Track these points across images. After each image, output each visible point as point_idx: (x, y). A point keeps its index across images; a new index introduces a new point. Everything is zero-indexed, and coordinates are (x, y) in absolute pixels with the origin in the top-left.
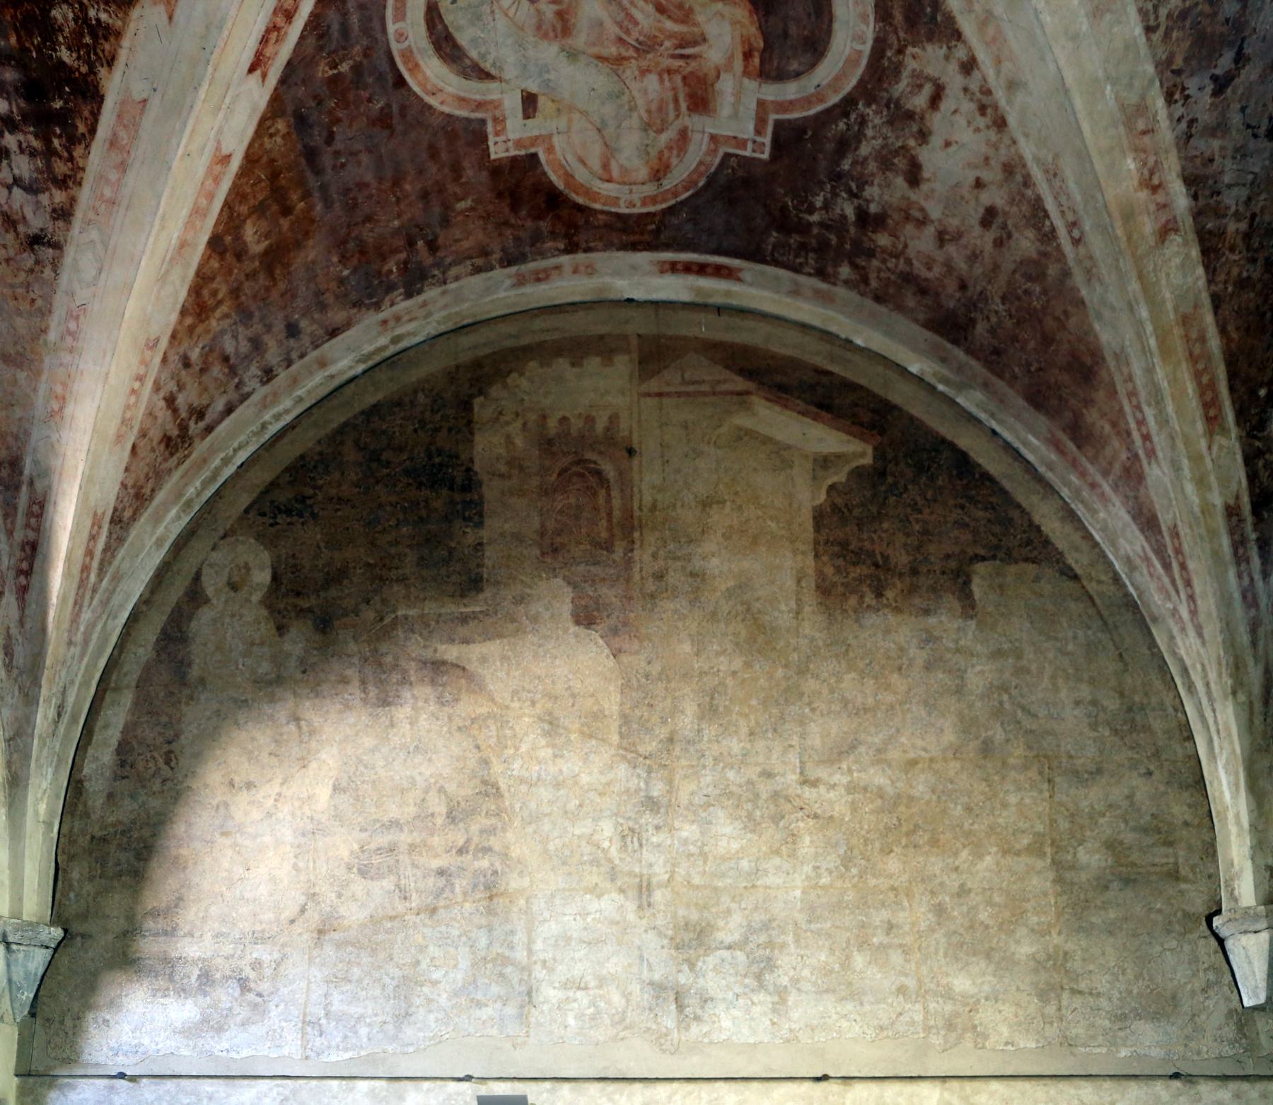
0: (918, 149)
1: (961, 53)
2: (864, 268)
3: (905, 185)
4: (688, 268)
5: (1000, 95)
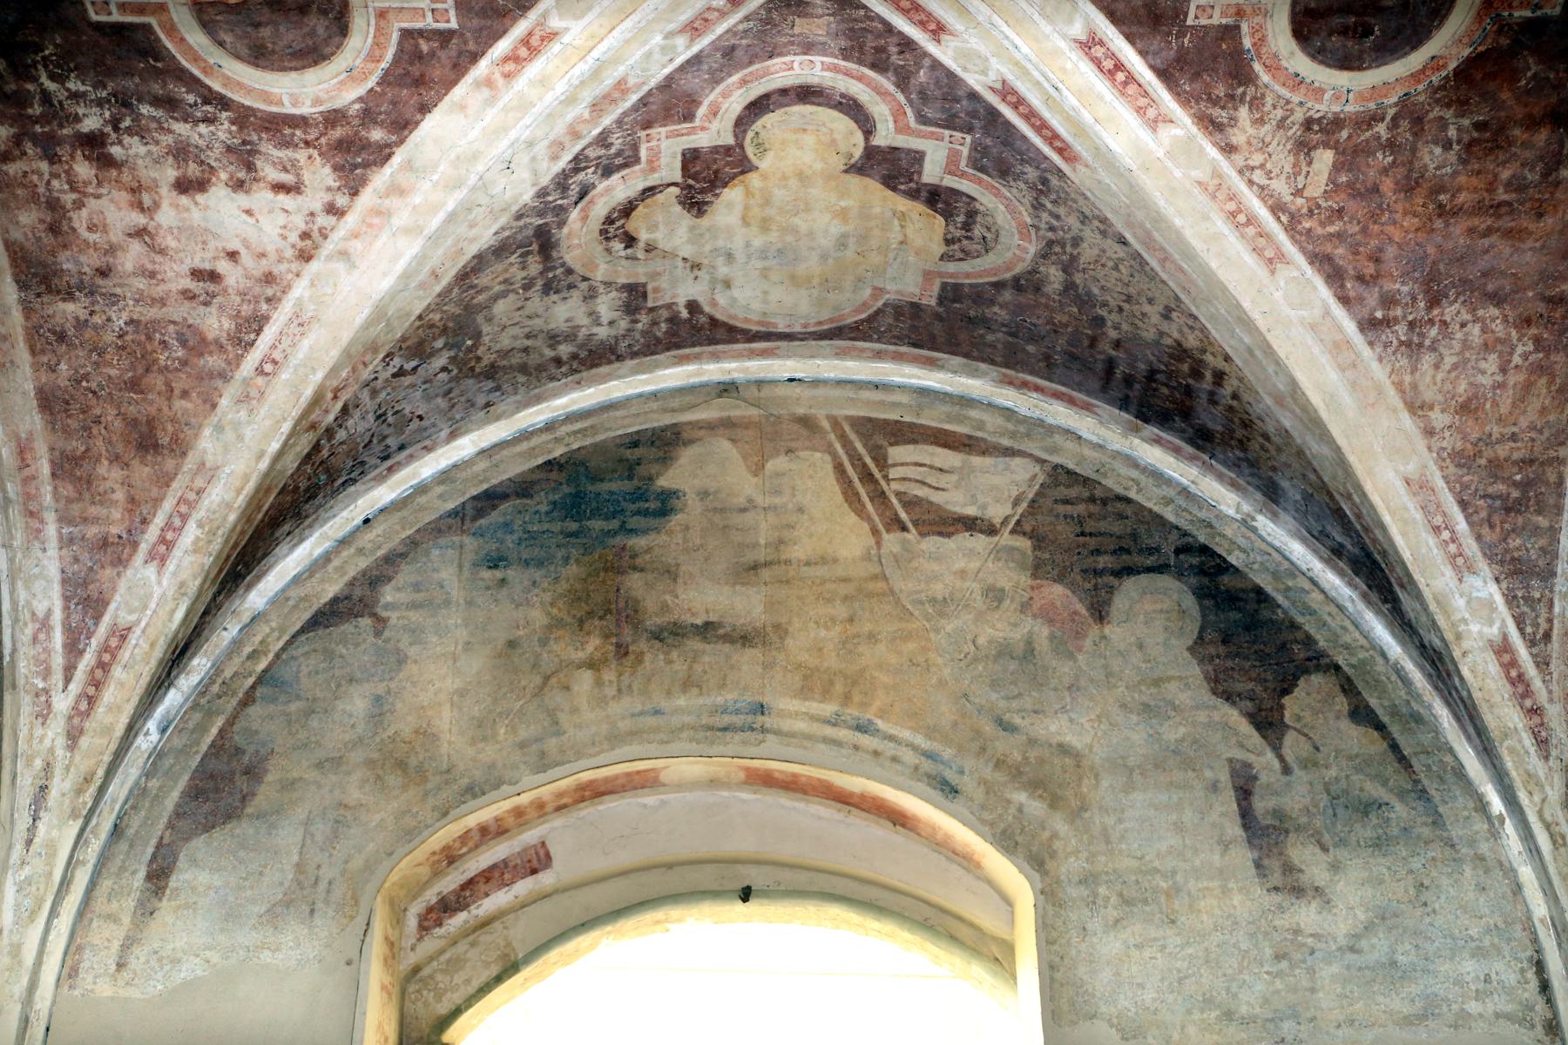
0: (222, 185)
1: (341, 200)
3: (172, 180)
5: (328, 247)
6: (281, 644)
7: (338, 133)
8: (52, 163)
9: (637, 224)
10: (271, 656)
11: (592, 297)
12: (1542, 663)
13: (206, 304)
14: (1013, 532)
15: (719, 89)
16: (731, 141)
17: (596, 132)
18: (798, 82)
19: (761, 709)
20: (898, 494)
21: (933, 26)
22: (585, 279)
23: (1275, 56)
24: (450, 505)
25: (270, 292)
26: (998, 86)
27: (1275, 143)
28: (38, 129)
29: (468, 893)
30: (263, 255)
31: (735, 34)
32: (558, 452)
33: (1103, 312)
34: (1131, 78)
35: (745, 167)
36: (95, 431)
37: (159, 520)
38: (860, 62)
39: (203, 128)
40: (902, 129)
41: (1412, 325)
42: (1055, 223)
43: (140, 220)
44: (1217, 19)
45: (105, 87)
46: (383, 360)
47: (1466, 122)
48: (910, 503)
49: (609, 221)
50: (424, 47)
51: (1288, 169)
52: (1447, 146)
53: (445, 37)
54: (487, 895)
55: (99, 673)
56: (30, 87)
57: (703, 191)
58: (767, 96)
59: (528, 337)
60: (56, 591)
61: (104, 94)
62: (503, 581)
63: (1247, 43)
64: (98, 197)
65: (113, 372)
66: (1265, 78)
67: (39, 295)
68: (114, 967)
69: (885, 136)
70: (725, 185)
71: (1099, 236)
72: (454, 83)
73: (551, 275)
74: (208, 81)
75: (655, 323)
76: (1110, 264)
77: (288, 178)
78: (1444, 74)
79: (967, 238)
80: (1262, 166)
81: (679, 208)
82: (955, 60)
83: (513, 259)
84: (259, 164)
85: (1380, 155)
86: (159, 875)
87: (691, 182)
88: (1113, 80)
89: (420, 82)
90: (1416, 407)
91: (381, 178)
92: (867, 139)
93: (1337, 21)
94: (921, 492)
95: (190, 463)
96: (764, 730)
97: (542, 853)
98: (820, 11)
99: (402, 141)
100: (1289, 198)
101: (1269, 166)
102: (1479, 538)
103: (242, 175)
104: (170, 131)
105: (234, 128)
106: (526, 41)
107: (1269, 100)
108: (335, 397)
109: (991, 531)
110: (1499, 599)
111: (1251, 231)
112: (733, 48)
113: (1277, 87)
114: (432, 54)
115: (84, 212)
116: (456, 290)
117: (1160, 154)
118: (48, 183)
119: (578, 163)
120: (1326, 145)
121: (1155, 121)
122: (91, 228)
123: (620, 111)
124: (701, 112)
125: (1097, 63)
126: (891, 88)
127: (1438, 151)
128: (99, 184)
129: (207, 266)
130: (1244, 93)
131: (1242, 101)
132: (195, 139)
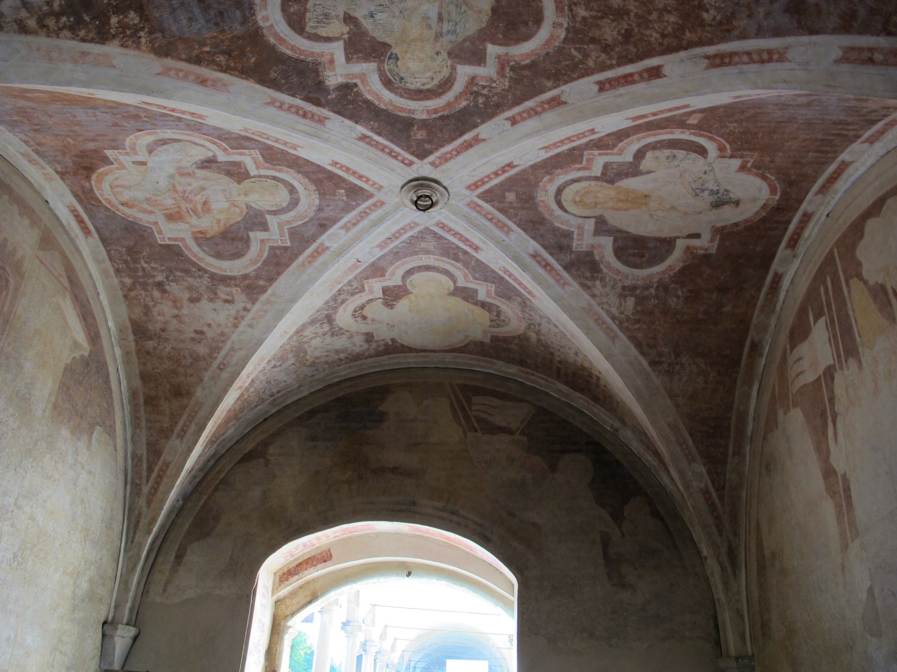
2: (136, 288)
4: (77, 217)
5: (244, 323)
6: (230, 467)
7: (247, 282)
8: (145, 291)
9: (366, 312)
10: (225, 472)
11: (351, 337)
12: (721, 498)
13: (199, 342)
14: (520, 434)
15: (393, 266)
16: (400, 283)
17: (346, 281)
18: (425, 264)
19: (414, 503)
20: (475, 417)
22: (348, 331)
23: (609, 263)
24: (297, 415)
25: (223, 339)
27: (611, 294)
28: (141, 280)
29: (299, 568)
30: (220, 325)
31: (398, 248)
32: (341, 394)
33: (553, 350)
34: (552, 268)
35: (407, 292)
36: (159, 388)
37: (181, 423)
38: (449, 258)
39: (198, 280)
41: (669, 365)
42: (530, 317)
43: (176, 312)
44: (584, 249)
45: (163, 266)
46: (267, 363)
47: (685, 290)
48: (480, 420)
49: (355, 311)
50: (278, 252)
51: (617, 303)
52: (678, 297)
54: (306, 569)
55: (158, 480)
56: (138, 266)
57: (392, 301)
58: (413, 268)
59: (327, 352)
60: (144, 447)
61: (164, 268)
62: (316, 446)
63: (597, 258)
64: (161, 303)
65: (166, 366)
66: (605, 270)
67: (141, 338)
68: (161, 591)
69: (461, 283)
70: (401, 298)
73: (333, 330)
74: (200, 264)
75: (378, 346)
77: (229, 298)
78: (674, 271)
79: (498, 320)
81: (383, 306)
83: (317, 325)
84: (218, 293)
85: (653, 300)
86: (179, 557)
87: (386, 297)
89: (278, 264)
90: (672, 395)
91: (263, 298)
93: (631, 251)
94: (484, 416)
95: (192, 402)
96: (414, 512)
97: (329, 554)
99: (271, 285)
101: (610, 303)
102: (697, 448)
103: (212, 296)
104: (186, 281)
105: (209, 280)
106: (316, 251)
107: (607, 279)
108: (248, 377)
109: (511, 433)
110: (704, 472)
111: (604, 326)
112: (398, 253)
113: (610, 274)
115: (157, 309)
116: (295, 337)
118: (144, 298)
120: (631, 296)
121: (564, 284)
122: (159, 315)
123: (355, 274)
124: (387, 274)
125: (539, 263)
126: (462, 267)
127: (675, 299)
128: (162, 299)
129: (200, 329)
130: (598, 276)
131: (597, 278)
132: (195, 284)
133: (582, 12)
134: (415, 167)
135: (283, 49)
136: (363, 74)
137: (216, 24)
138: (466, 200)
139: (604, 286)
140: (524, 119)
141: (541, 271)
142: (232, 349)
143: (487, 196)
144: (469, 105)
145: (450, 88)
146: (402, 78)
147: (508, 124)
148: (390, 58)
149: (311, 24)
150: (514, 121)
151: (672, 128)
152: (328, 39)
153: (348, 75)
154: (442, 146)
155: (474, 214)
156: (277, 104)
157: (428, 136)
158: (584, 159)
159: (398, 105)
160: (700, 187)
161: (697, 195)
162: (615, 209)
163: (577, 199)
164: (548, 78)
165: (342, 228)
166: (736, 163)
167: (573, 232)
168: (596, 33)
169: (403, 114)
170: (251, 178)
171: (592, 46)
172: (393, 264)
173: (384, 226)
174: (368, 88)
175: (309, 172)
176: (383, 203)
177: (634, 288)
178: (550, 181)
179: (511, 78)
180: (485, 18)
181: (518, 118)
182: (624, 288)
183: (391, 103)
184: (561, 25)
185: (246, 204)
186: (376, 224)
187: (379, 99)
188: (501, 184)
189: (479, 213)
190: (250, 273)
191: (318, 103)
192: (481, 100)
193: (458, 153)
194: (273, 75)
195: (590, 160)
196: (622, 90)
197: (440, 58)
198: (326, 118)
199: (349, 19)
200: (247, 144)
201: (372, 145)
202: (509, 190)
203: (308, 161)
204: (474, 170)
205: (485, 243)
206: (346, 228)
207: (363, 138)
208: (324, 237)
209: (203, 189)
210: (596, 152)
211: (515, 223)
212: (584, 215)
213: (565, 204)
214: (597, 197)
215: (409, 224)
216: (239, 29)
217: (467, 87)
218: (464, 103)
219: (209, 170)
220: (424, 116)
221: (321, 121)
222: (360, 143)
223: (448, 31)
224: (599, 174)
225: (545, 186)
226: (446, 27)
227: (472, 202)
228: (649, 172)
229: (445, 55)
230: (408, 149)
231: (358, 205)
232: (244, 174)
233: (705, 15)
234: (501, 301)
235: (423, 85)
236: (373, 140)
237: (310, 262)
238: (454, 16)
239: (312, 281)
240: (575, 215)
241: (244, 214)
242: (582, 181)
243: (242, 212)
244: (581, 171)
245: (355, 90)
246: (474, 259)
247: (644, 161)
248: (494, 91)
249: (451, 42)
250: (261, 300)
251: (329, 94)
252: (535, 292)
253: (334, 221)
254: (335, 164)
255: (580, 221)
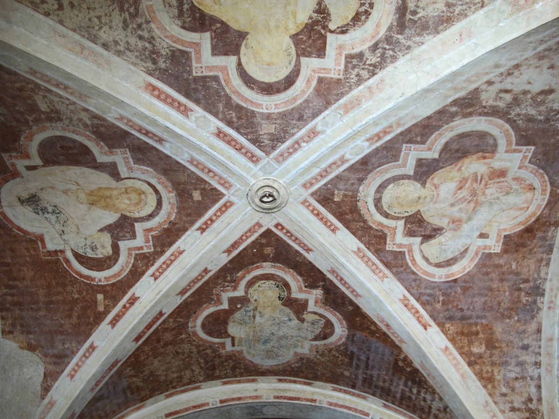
15: (306, 97)
16: (303, 60)
17: (361, 87)
21: (221, 135)
23: (89, 140)
26: (189, 113)
31: (298, 127)
38: (247, 110)
40: (224, 69)
42: (140, 32)
50: (419, 139)
53: (410, 141)
58: (286, 89)
63: (102, 143)
71: (117, 39)
72: (413, 125)
76: (103, 20)
77: (502, 95)
80: (67, 105)
82: (210, 121)
83: (421, 14)
88: (146, 130)
92: (239, 59)
93: (75, 151)
98: (265, 137)
99: (444, 107)
100: (47, 94)
105: (511, 112)
106: (379, 138)
114: (417, 136)
117: (113, 108)
119: (374, 70)
123: (349, 96)
124: (314, 83)
125: (154, 135)
126: (233, 96)
130: (92, 128)
131: (91, 126)
133: (183, 336)
134: (274, 222)
135: (340, 317)
136: (300, 292)
137: (367, 340)
138: (233, 191)
139: (80, 120)
140: (200, 275)
141: (150, 128)
142: (542, 42)
143: (215, 196)
144: (236, 274)
145: (248, 282)
146: (277, 287)
147: (209, 268)
148: (283, 299)
149: (322, 322)
150: (206, 271)
151: (108, 285)
152: (315, 313)
153: (309, 293)
154: (253, 242)
155: (225, 176)
156: (355, 293)
157: (263, 250)
158: (151, 242)
159: (281, 271)
160: (58, 215)
161: (55, 206)
162: (110, 188)
163: (143, 196)
164: (191, 302)
165: (347, 161)
166: (51, 246)
167: (135, 164)
168: (173, 333)
169: (279, 265)
170: (406, 217)
171: (173, 326)
172: (306, 101)
173: (306, 162)
174: (299, 284)
175: (357, 222)
176: (305, 186)
177: (50, 119)
178: (169, 215)
179: (212, 295)
180: (231, 319)
181: (204, 274)
182: (60, 120)
183: (286, 272)
184: (192, 328)
185: (424, 187)
186: (315, 164)
187: (293, 276)
188: (207, 209)
189: (221, 178)
190: (460, 119)
191: (331, 281)
192: (229, 278)
193: (241, 238)
194: (351, 308)
195: (147, 241)
196: (150, 320)
197: (255, 297)
198: (329, 271)
199: (302, 321)
200: (390, 258)
201: (303, 243)
202: (199, 202)
203: (354, 234)
204: (229, 224)
205: (212, 147)
206: (343, 160)
207: (308, 250)
208: (367, 152)
209: (452, 205)
210: (145, 250)
211: (188, 169)
212: (132, 180)
213: (151, 190)
214: (129, 199)
215: (284, 160)
216: (359, 334)
217: (238, 284)
218: (239, 274)
219: (435, 227)
220: (265, 264)
221: (333, 271)
222: (311, 247)
223: (250, 311)
224: (136, 225)
225: (172, 208)
226: (251, 314)
227: (227, 188)
228: (101, 230)
229: (252, 300)
230: (279, 239)
231: (326, 185)
232: (409, 222)
233: (130, 368)
234: (183, 43)
235: (264, 283)
236: (302, 247)
237: (391, 127)
238: (247, 318)
239: (398, 108)
240: (139, 180)
241: (432, 177)
242: (146, 217)
243: (433, 179)
244: (150, 227)
245: (307, 284)
246: (220, 116)
247: (111, 243)
248: (221, 286)
249: (248, 307)
250: (467, 92)
251: (323, 286)
252: (147, 97)
253: (352, 168)
254: (334, 230)
255: (132, 175)
